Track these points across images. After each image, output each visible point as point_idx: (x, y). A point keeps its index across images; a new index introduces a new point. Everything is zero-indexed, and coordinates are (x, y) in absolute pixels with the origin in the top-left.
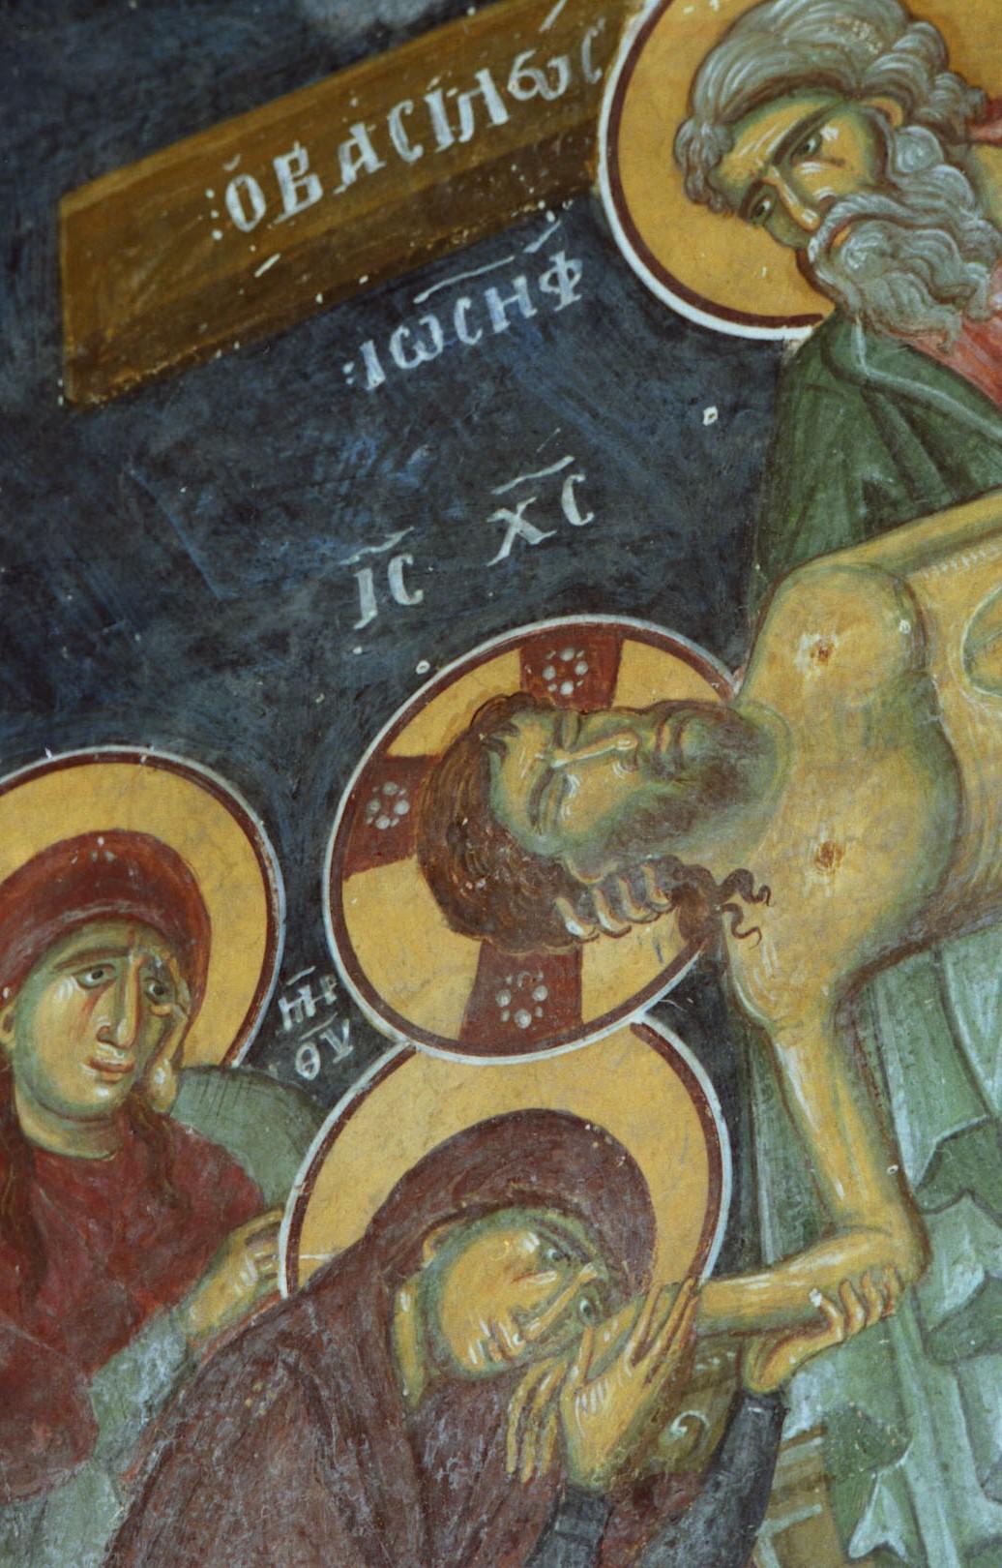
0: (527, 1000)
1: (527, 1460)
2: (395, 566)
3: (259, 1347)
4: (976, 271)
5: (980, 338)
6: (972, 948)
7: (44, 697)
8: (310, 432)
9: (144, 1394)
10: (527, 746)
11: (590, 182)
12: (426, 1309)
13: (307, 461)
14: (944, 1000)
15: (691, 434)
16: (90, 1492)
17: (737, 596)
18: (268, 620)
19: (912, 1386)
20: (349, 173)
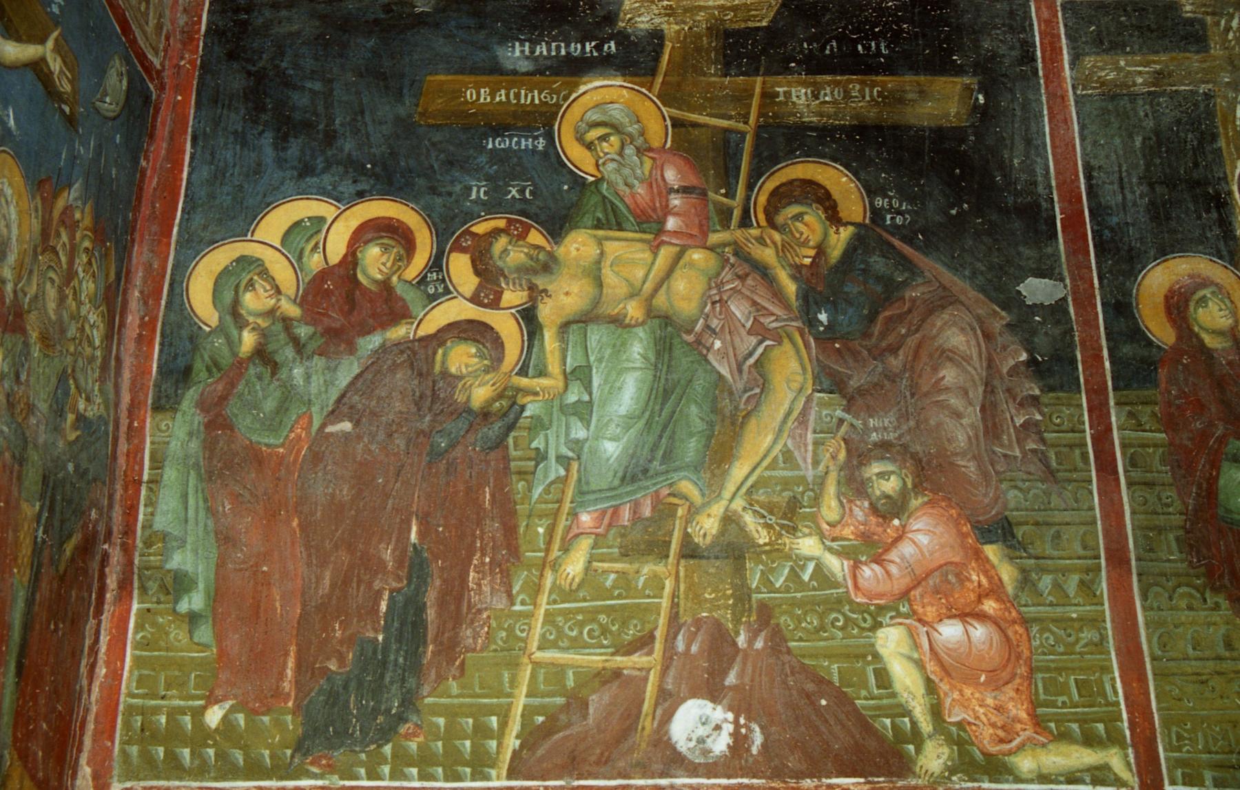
1: (460, 398)
2: (482, 190)
3: (402, 347)
4: (636, 182)
5: (633, 197)
6: (595, 327)
7: (390, 183)
8: (471, 151)
9: (371, 347)
10: (503, 241)
11: (553, 125)
12: (444, 355)
13: (469, 157)
14: (586, 336)
15: (560, 190)
16: (351, 364)
17: (561, 229)
18: (449, 189)
20: (498, 99)
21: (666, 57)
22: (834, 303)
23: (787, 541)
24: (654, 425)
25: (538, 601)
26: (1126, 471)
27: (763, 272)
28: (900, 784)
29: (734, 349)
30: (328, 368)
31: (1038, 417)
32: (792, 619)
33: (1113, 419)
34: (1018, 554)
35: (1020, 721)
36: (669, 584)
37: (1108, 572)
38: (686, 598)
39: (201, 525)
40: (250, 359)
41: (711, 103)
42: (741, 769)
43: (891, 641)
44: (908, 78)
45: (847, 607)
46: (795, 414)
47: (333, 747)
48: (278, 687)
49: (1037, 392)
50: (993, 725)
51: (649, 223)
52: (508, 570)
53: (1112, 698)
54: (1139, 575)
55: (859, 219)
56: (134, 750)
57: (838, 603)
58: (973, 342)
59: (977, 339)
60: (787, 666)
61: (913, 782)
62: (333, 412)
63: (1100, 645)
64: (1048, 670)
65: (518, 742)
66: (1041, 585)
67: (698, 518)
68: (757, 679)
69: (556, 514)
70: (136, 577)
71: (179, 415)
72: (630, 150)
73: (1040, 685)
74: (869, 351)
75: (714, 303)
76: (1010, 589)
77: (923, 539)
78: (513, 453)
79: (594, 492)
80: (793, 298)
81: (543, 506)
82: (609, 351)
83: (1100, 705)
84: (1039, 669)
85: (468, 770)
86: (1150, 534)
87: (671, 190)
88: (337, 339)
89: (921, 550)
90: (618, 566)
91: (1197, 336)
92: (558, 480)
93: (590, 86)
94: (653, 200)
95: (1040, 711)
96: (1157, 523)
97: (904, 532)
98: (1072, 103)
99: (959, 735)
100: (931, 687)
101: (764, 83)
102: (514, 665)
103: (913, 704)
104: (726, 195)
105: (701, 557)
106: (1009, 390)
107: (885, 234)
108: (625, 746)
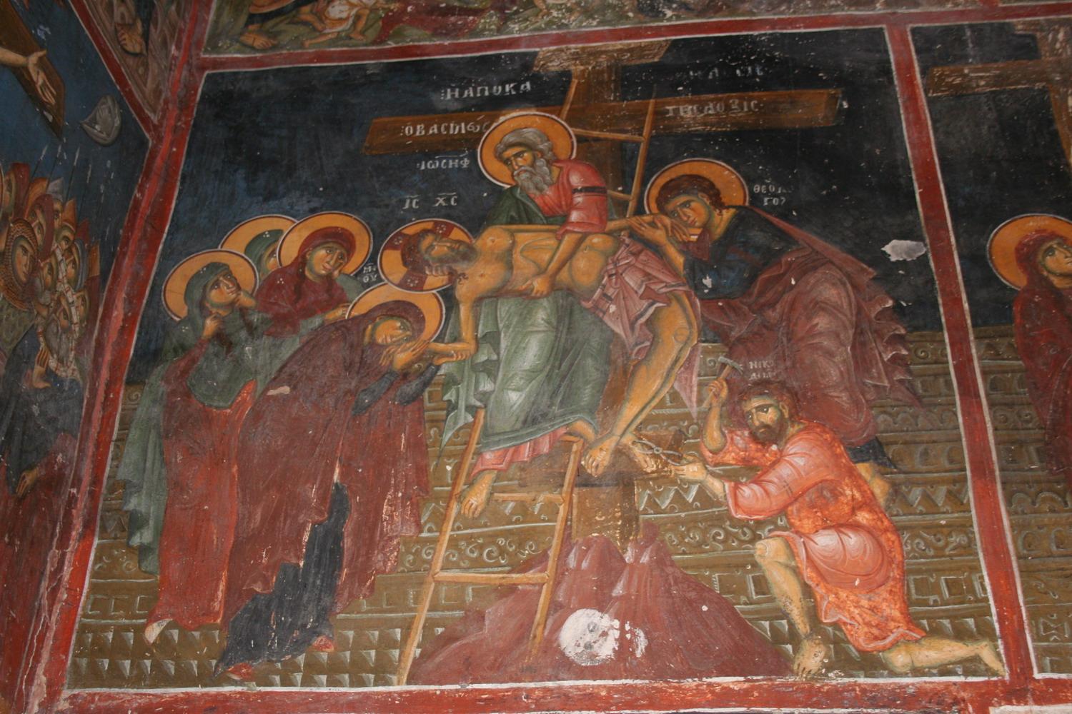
0: (414, 279)
1: (384, 362)
4: (545, 187)
10: (429, 239)
14: (496, 307)
16: (294, 340)
17: (480, 226)
19: (466, 373)
20: (431, 132)
21: (573, 90)
22: (717, 271)
23: (673, 468)
24: (554, 376)
25: (444, 529)
26: (987, 395)
27: (655, 249)
28: (778, 681)
29: (627, 311)
30: (274, 345)
31: (904, 352)
32: (676, 535)
33: (974, 351)
34: (889, 470)
35: (893, 620)
36: (562, 510)
37: (974, 482)
38: (579, 521)
39: (156, 473)
40: (209, 340)
41: (613, 123)
42: (626, 670)
43: (769, 550)
44: (780, 92)
45: (728, 523)
46: (682, 361)
47: (254, 658)
48: (209, 605)
49: (903, 332)
50: (868, 624)
51: (556, 218)
52: (418, 504)
53: (980, 595)
54: (1003, 483)
55: (740, 203)
56: (84, 662)
57: (718, 520)
58: (843, 294)
59: (847, 292)
60: (671, 577)
61: (791, 680)
62: (275, 379)
63: (968, 548)
64: (919, 572)
65: (419, 651)
66: (911, 497)
67: (591, 452)
68: (642, 590)
69: (463, 454)
70: (99, 517)
71: (147, 388)
72: (540, 162)
73: (912, 586)
74: (750, 307)
75: (610, 276)
76: (882, 501)
77: (800, 462)
78: (427, 404)
79: (499, 434)
80: (681, 267)
81: (452, 448)
82: (515, 319)
83: (970, 602)
84: (911, 572)
85: (372, 676)
86: (1012, 447)
87: (575, 191)
88: (283, 323)
89: (799, 474)
90: (517, 496)
91: (1046, 279)
92: (467, 426)
93: (508, 116)
94: (559, 197)
95: (913, 609)
96: (1018, 437)
97: (782, 456)
98: (925, 104)
99: (835, 634)
100: (807, 591)
101: (656, 104)
102: (421, 583)
103: (791, 607)
104: (622, 192)
105: (593, 486)
106: (876, 331)
107: (763, 214)
108: (516, 653)
